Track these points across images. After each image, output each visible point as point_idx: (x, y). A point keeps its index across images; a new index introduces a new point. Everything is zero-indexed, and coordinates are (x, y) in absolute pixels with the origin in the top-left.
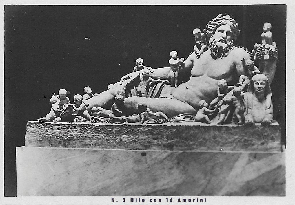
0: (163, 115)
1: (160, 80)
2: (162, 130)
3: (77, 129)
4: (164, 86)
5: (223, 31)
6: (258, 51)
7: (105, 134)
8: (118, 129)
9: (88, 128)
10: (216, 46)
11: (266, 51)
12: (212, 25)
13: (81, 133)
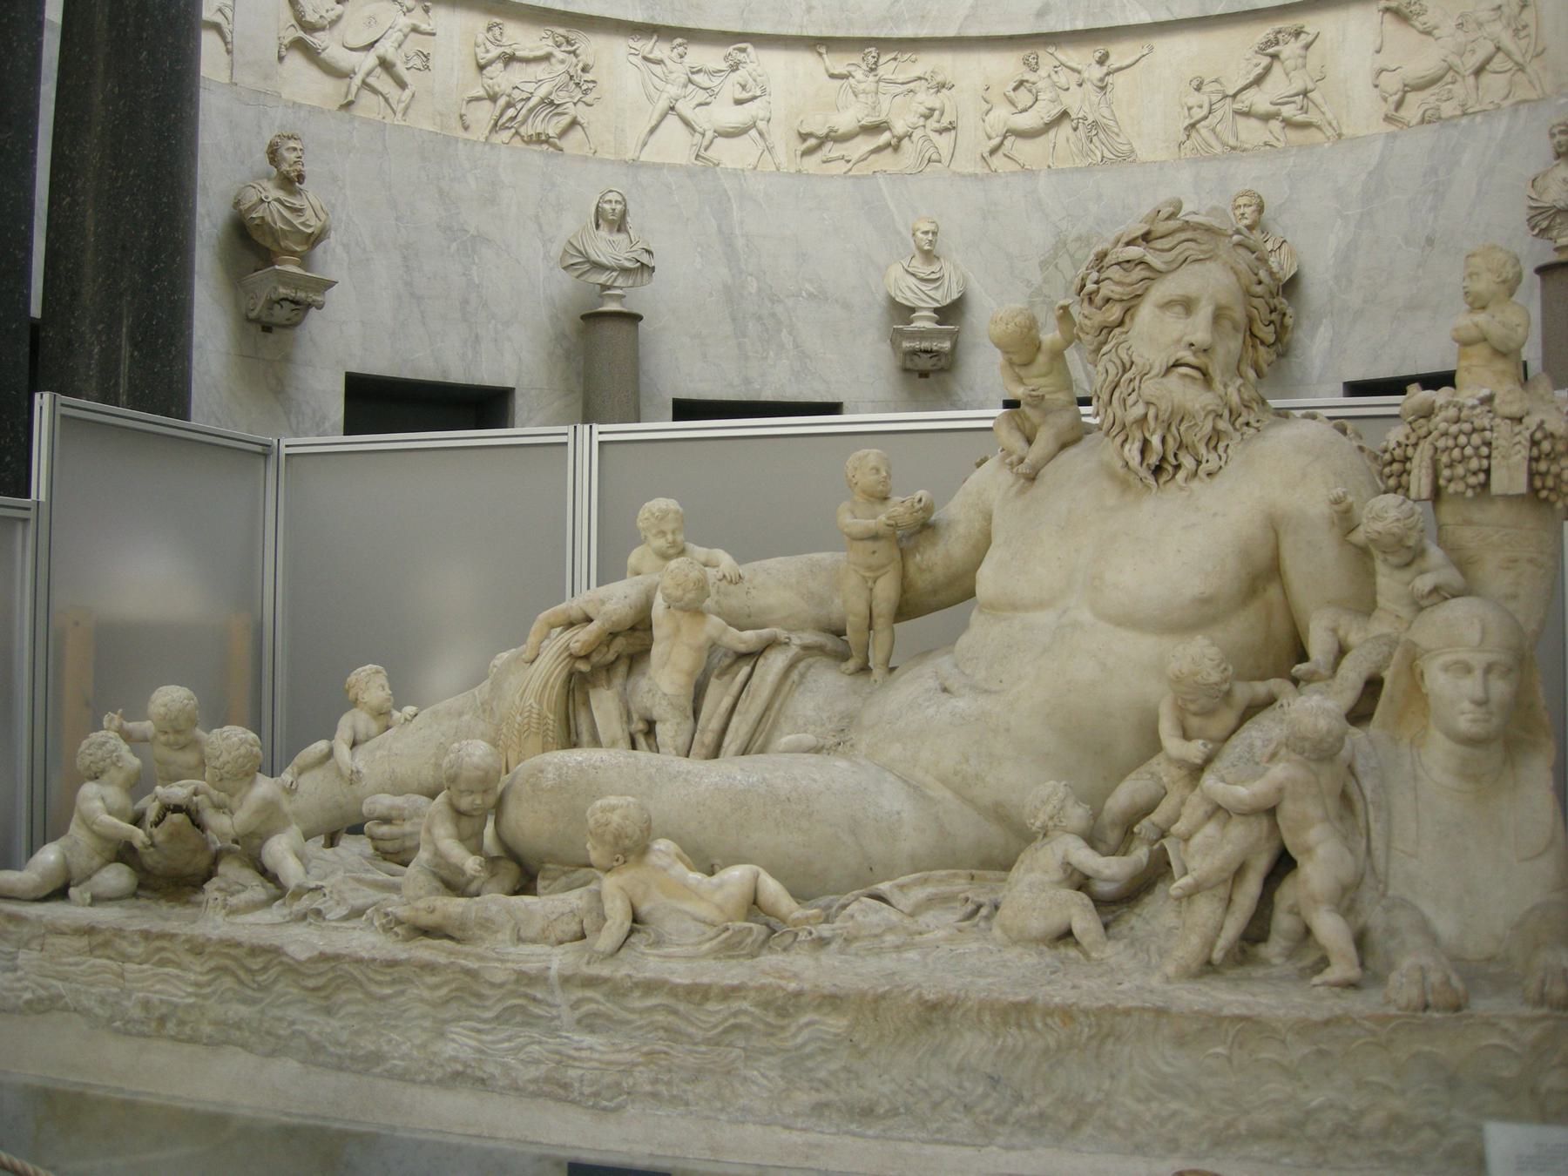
0: (772, 888)
1: (782, 634)
2: (745, 1020)
3: (178, 965)
4: (801, 666)
5: (1188, 305)
6: (1445, 434)
7: (353, 1015)
8: (436, 987)
9: (249, 971)
10: (1148, 404)
11: (1502, 434)
12: (1115, 273)
13: (206, 997)
